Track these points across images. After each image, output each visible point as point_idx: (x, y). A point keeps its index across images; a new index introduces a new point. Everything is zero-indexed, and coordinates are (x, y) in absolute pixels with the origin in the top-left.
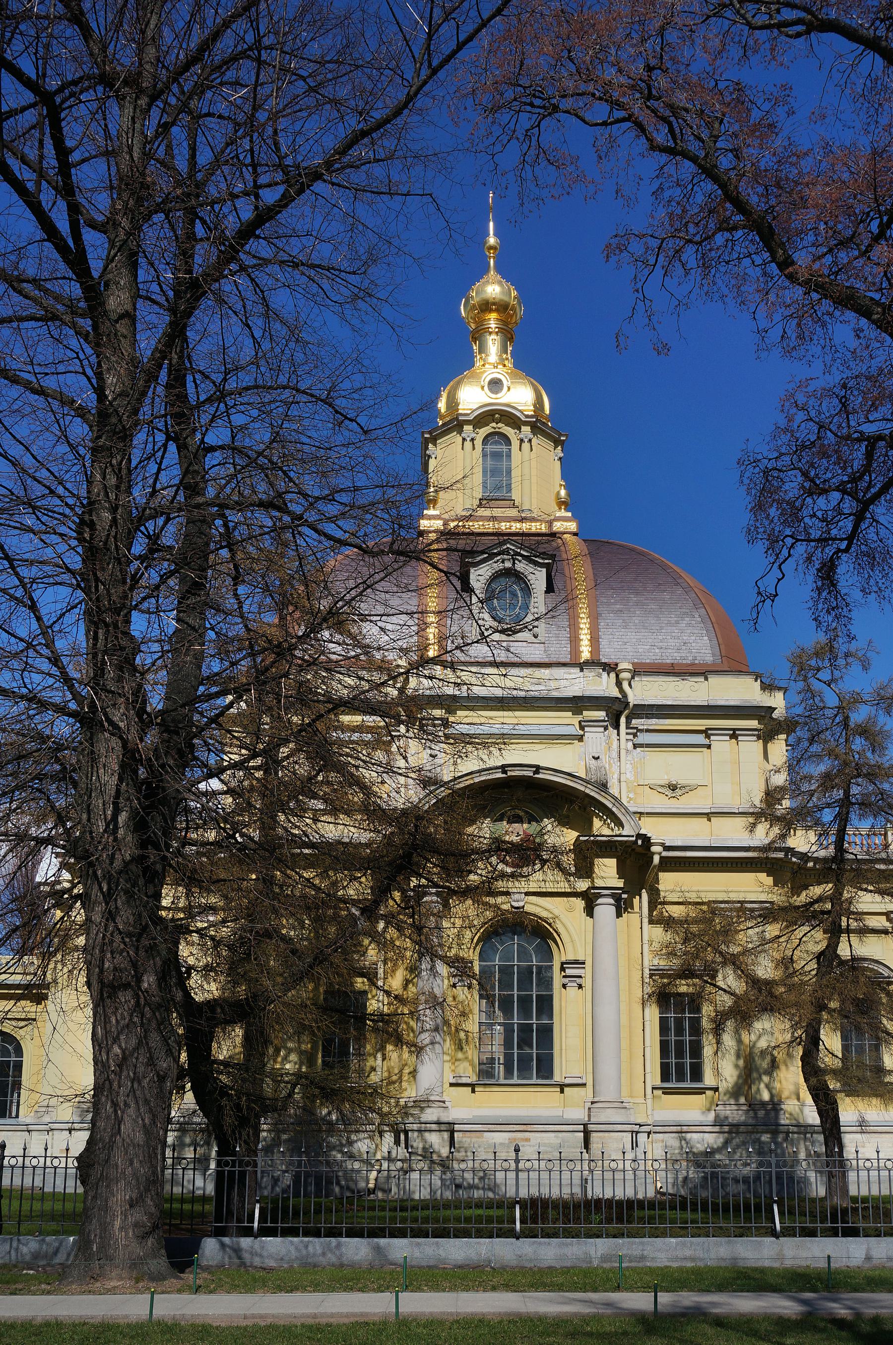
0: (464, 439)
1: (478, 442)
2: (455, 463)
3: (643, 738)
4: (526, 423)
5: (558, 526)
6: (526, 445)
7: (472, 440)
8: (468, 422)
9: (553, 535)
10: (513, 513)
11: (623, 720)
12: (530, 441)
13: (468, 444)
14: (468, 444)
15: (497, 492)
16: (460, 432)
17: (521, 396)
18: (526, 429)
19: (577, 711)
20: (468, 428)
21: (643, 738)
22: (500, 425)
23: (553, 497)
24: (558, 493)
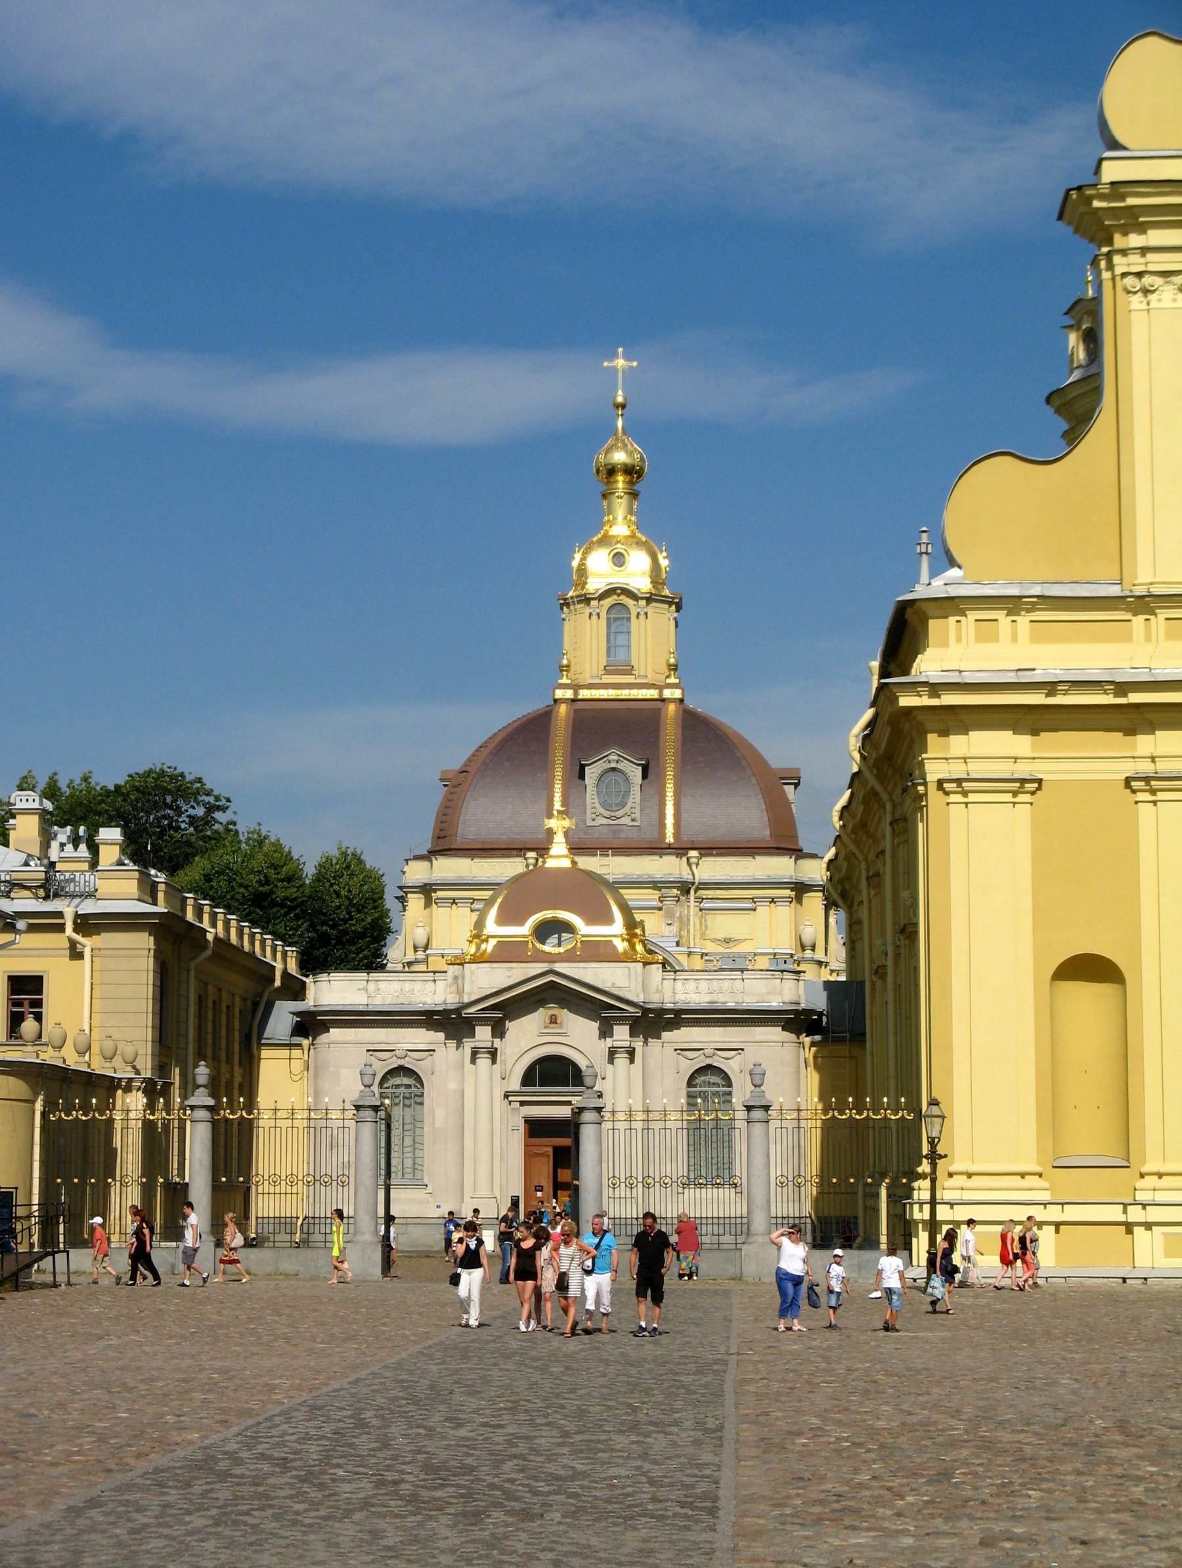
0: (591, 614)
1: (603, 615)
2: (584, 640)
3: (705, 905)
4: (642, 598)
5: (667, 693)
6: (642, 617)
7: (598, 614)
8: (594, 599)
9: (663, 700)
11: (692, 892)
12: (646, 614)
13: (594, 617)
14: (594, 617)
15: (619, 666)
16: (589, 604)
17: (637, 572)
18: (643, 603)
19: (659, 889)
20: (594, 603)
21: (705, 905)
22: (622, 597)
23: (664, 663)
24: (668, 661)
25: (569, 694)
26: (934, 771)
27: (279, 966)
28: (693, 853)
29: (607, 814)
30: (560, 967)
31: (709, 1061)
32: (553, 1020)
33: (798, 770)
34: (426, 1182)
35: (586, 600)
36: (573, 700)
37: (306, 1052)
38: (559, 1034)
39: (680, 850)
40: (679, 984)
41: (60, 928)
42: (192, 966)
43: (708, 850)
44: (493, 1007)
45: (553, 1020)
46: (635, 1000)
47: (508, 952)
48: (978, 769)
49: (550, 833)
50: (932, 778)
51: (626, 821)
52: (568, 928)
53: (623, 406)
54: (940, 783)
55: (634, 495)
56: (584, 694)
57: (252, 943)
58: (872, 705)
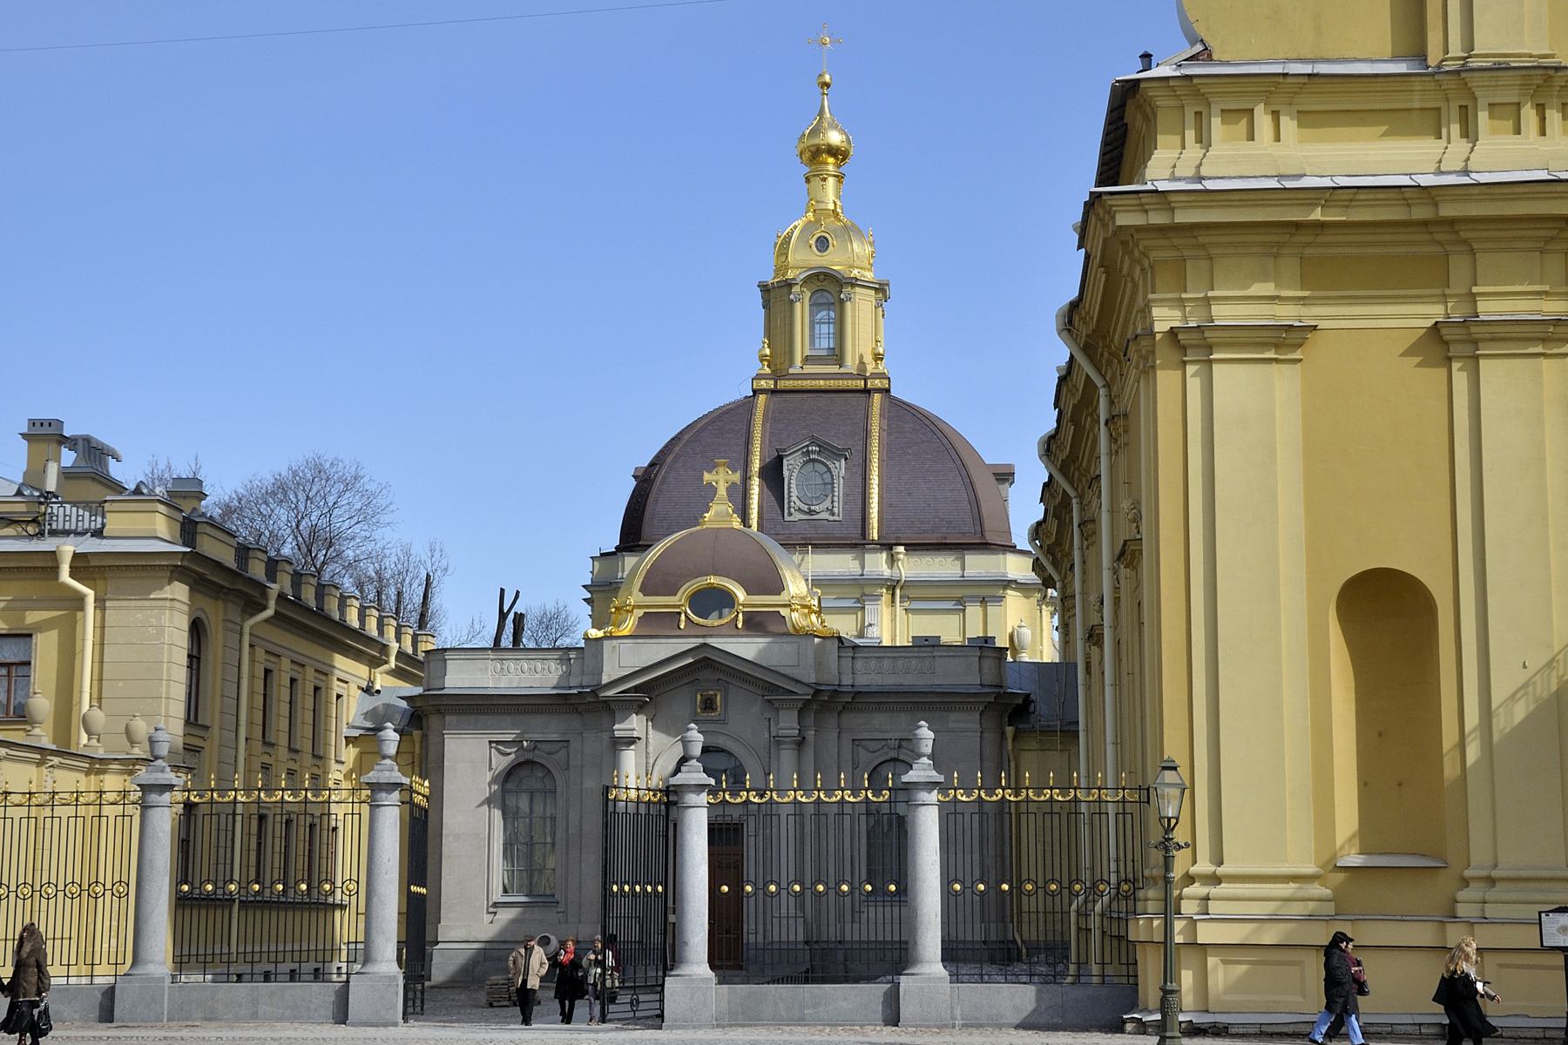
10: (834, 369)
20: (796, 289)
25: (771, 384)
26: (1164, 318)
27: (394, 646)
28: (901, 549)
29: (805, 508)
30: (713, 642)
31: (893, 754)
32: (709, 705)
33: (1010, 466)
34: (557, 897)
35: (789, 285)
36: (773, 392)
37: (417, 745)
38: (716, 722)
39: (887, 546)
40: (859, 664)
41: (55, 570)
42: (247, 630)
43: (912, 547)
44: (636, 689)
45: (709, 705)
46: (806, 680)
47: (655, 624)
48: (1225, 314)
49: (712, 490)
50: (1161, 327)
51: (825, 515)
52: (727, 599)
53: (828, 85)
54: (1173, 332)
55: (840, 178)
56: (782, 384)
57: (362, 617)
58: (1079, 248)
